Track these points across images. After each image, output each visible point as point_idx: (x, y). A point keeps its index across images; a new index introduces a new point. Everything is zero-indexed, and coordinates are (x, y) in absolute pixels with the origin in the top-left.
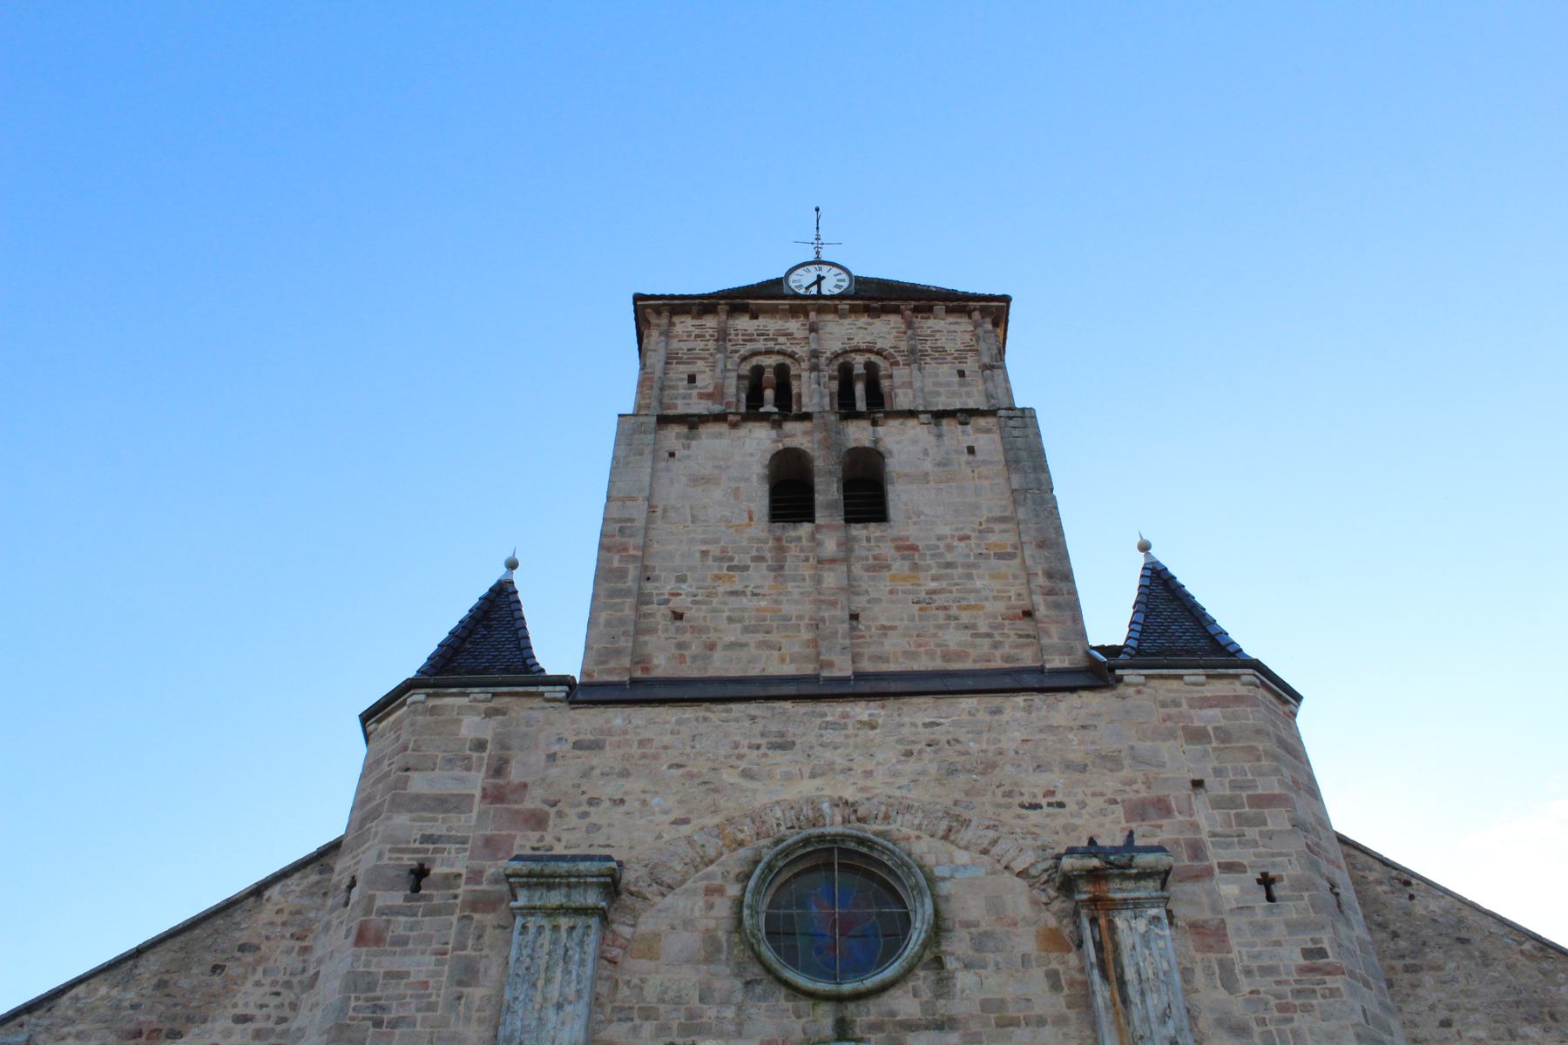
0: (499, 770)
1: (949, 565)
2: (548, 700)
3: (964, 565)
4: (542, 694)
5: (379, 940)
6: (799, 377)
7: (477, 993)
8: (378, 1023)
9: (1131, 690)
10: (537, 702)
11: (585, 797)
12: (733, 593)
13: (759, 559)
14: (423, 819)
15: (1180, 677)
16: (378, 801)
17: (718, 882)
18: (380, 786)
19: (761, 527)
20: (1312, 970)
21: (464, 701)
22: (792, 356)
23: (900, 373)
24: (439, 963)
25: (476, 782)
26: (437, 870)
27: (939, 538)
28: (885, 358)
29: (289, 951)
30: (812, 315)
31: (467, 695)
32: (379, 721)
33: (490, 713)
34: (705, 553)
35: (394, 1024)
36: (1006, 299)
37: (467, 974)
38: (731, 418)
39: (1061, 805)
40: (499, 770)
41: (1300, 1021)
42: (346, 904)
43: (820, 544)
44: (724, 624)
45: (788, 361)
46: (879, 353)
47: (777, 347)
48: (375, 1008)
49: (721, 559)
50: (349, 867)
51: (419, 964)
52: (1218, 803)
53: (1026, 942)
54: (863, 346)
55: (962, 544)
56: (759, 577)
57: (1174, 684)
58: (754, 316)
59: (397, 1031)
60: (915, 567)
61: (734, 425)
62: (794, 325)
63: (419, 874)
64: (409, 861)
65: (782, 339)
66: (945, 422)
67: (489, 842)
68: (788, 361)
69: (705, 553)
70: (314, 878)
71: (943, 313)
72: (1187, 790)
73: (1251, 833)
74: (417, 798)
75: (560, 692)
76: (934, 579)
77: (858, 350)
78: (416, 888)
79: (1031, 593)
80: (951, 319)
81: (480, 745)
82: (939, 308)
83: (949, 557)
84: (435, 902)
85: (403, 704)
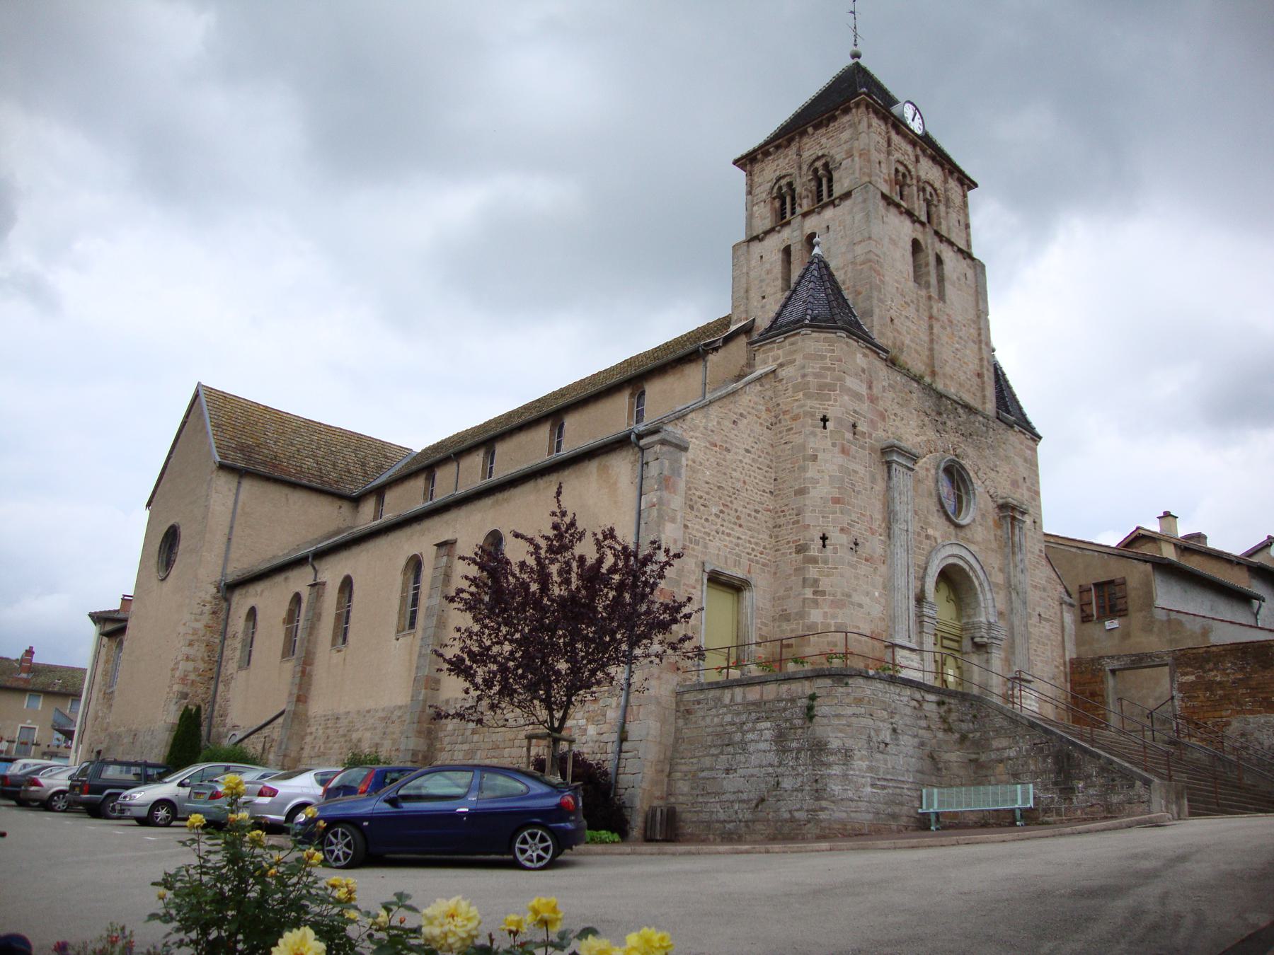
0: (870, 387)
1: (960, 338)
2: (880, 357)
3: (965, 341)
4: (878, 354)
5: (848, 455)
6: (909, 186)
7: (877, 488)
8: (854, 491)
9: (1014, 433)
10: (875, 356)
11: (893, 412)
12: (907, 317)
13: (912, 302)
14: (852, 401)
15: (1024, 434)
16: (828, 380)
17: (928, 467)
18: (829, 373)
19: (911, 284)
20: (1040, 556)
21: (856, 344)
22: (909, 172)
23: (942, 208)
24: (866, 471)
25: (863, 390)
26: (859, 428)
27: (958, 321)
28: (937, 194)
29: (756, 423)
30: (918, 149)
31: (858, 342)
32: (813, 331)
33: (865, 355)
34: (897, 288)
35: (859, 492)
36: (976, 185)
37: (873, 480)
38: (902, 209)
39: (998, 472)
40: (870, 387)
41: (1037, 572)
42: (825, 427)
43: (931, 307)
44: (905, 333)
45: (907, 173)
46: (935, 190)
47: (905, 162)
48: (852, 484)
49: (902, 295)
50: (819, 409)
51: (862, 471)
52: (1029, 489)
53: (991, 523)
54: (931, 182)
55: (964, 328)
56: (911, 311)
57: (1023, 436)
58: (898, 133)
59: (860, 496)
60: (953, 334)
61: (901, 213)
62: (909, 148)
63: (854, 426)
64: (851, 420)
65: (906, 157)
66: (959, 254)
67: (872, 421)
68: (907, 173)
69: (897, 288)
70: (759, 388)
71: (955, 178)
72: (1022, 480)
73: (1033, 503)
74: (850, 389)
75: (883, 355)
76: (958, 343)
77: (928, 183)
78: (854, 434)
79: (982, 367)
80: (956, 183)
81: (863, 371)
82: (956, 175)
83: (960, 333)
84: (861, 443)
85: (836, 333)
